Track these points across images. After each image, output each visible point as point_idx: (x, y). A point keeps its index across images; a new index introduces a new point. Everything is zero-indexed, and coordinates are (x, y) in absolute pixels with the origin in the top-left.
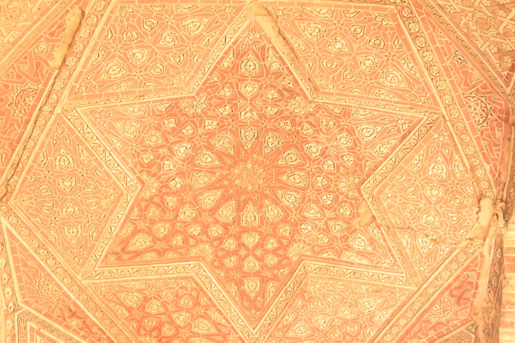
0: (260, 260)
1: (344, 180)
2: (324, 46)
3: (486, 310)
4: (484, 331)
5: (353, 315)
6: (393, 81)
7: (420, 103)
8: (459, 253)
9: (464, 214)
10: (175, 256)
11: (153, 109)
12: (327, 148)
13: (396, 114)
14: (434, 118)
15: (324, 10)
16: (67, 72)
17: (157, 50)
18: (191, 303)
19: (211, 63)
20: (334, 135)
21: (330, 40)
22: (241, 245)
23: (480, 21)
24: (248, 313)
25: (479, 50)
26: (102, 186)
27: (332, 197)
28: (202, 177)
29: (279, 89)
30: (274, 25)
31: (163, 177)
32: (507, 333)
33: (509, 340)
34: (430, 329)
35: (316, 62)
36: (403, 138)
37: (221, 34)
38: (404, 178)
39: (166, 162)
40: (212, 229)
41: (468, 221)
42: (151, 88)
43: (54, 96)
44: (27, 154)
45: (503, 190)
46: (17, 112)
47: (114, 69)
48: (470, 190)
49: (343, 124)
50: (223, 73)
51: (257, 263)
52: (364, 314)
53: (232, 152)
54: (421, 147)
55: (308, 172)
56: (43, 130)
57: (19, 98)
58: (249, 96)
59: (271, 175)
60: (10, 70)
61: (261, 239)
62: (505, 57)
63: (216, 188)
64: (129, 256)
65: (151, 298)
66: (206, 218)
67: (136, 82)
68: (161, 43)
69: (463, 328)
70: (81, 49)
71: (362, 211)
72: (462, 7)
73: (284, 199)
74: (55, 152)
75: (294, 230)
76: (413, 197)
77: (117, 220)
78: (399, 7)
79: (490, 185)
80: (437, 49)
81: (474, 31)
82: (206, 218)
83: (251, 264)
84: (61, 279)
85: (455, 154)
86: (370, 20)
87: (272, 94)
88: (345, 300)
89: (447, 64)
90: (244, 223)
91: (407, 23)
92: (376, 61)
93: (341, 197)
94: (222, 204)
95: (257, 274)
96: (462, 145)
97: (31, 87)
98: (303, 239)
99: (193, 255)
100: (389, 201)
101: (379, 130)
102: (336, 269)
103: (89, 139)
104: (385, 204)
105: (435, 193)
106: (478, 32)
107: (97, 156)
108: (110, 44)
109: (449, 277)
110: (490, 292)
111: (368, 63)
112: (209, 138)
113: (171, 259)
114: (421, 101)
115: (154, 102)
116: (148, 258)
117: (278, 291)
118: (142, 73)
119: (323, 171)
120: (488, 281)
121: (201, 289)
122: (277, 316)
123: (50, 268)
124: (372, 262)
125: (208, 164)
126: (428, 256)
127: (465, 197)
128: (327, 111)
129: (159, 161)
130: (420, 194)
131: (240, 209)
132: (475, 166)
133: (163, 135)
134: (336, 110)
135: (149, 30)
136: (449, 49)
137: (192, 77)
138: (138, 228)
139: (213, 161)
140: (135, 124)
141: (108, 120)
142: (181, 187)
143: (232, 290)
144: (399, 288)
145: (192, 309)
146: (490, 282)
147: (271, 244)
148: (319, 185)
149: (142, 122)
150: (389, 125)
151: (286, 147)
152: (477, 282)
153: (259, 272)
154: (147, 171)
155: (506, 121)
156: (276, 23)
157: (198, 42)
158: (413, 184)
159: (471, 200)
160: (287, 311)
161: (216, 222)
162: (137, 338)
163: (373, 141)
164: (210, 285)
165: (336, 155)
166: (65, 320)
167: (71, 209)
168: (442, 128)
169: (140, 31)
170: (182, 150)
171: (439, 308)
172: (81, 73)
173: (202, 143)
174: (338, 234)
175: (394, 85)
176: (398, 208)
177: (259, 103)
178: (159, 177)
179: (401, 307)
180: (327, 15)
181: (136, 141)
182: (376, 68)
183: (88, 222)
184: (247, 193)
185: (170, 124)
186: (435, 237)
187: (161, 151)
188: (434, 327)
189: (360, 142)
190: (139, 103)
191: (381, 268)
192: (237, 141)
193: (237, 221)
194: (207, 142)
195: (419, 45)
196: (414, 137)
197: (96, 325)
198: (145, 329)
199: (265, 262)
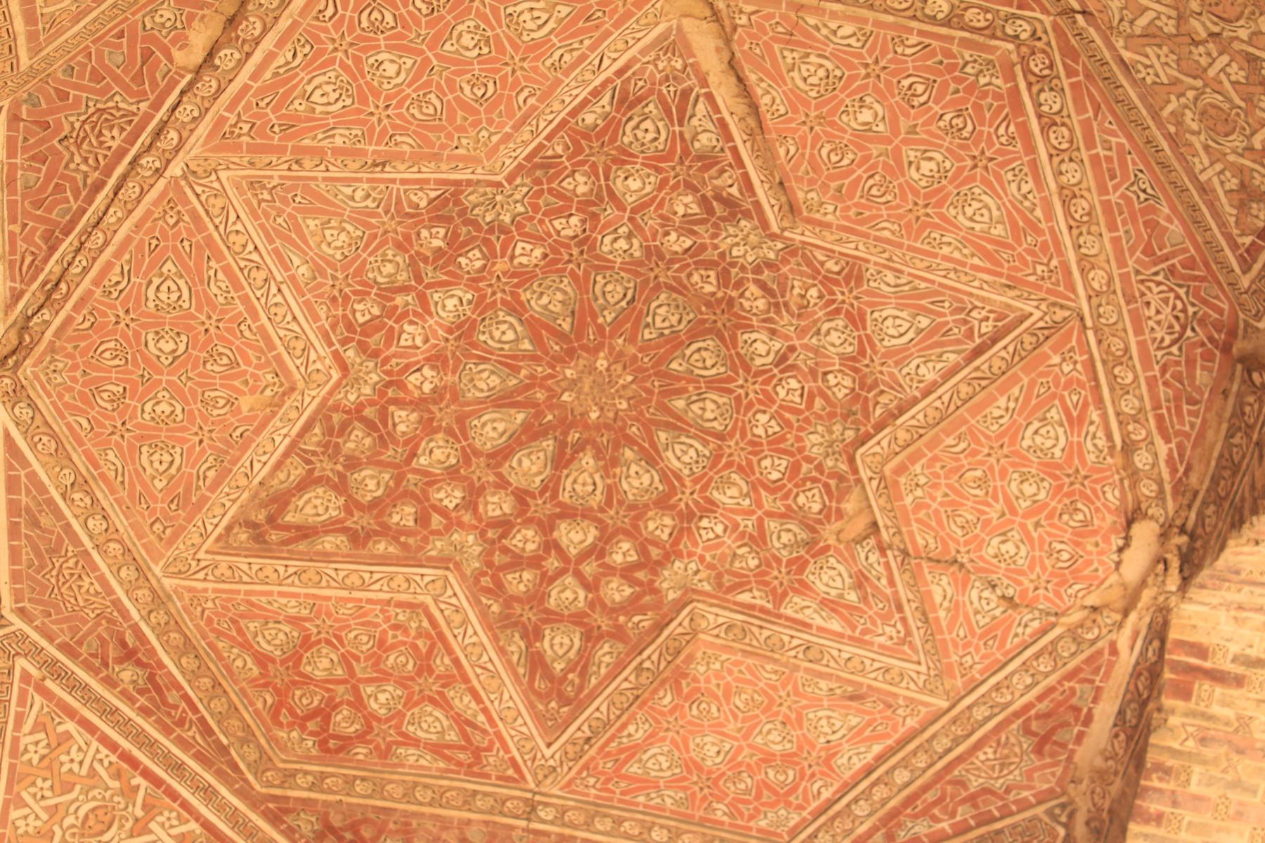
0: (590, 586)
1: (820, 428)
2: (832, 112)
3: (1101, 776)
4: (1087, 823)
5: (788, 746)
6: (977, 218)
7: (1032, 279)
8: (1060, 637)
10: (391, 549)
11: (399, 197)
12: (792, 349)
13: (971, 294)
14: (1058, 318)
15: (848, 29)
16: (214, 84)
17: (435, 62)
18: (410, 666)
19: (557, 111)
20: (816, 322)
21: (848, 101)
22: (551, 546)
23: (1212, 112)
24: (541, 707)
25: (1194, 178)
26: (248, 363)
27: (784, 463)
28: (485, 375)
29: (704, 196)
30: (721, 43)
31: (394, 361)
34: (964, 801)
35: (805, 147)
36: (978, 352)
37: (592, 48)
38: (963, 445)
39: (407, 327)
40: (490, 499)
41: (1096, 565)
42: (406, 148)
43: (173, 135)
44: (84, 263)
45: (1190, 507)
46: (77, 159)
47: (324, 93)
48: (1113, 496)
49: (840, 297)
50: (579, 139)
51: (582, 594)
52: (813, 746)
53: (566, 326)
54: (1015, 380)
55: (738, 399)
56: (130, 212)
57: (87, 127)
58: (630, 200)
59: (650, 392)
60: (79, 58)
61: (600, 539)
62: (1254, 205)
64: (285, 535)
65: (319, 642)
66: (480, 472)
67: (372, 129)
68: (447, 47)
69: (1039, 811)
70: (257, 33)
71: (849, 506)
72: (1176, 74)
73: (670, 454)
74: (151, 267)
75: (682, 529)
76: (977, 492)
77: (269, 448)
78: (1024, 49)
79: (1161, 491)
80: (1095, 160)
81: (1193, 133)
82: (480, 472)
83: (568, 594)
84: (114, 569)
85: (1092, 408)
86: (952, 68)
87: (685, 204)
89: (1114, 198)
90: (567, 495)
91: (1035, 89)
93: (805, 467)
94: (521, 444)
95: (578, 619)
96: (1112, 390)
97: (121, 105)
98: (699, 551)
99: (433, 553)
100: (919, 493)
101: (922, 326)
102: (766, 633)
103: (237, 248)
104: (908, 500)
105: (1029, 489)
106: (1202, 137)
107: (248, 290)
108: (326, 31)
109: (1028, 688)
110: (1116, 736)
111: (927, 167)
112: (517, 286)
113: (382, 556)
114: (1034, 273)
115: (404, 182)
116: (328, 546)
117: (619, 667)
118: (389, 112)
119: (773, 402)
120: (1116, 709)
122: (607, 724)
123: (91, 537)
124: (854, 628)
125: (507, 347)
126: (988, 632)
127: (1097, 510)
128: (809, 264)
129: (391, 323)
130: (995, 488)
131: (561, 460)
132: (1134, 442)
133: (412, 263)
134: (830, 265)
135: (425, 11)
136: (1123, 164)
137: (507, 138)
138: (317, 474)
139: (517, 340)
140: (349, 227)
141: (289, 210)
142: (434, 390)
143: (513, 648)
144: (905, 698)
145: (412, 679)
146: (1121, 713)
147: (624, 551)
148: (760, 431)
149: (367, 225)
150: (949, 318)
151: (698, 331)
152: (1090, 710)
154: (359, 342)
155: (1226, 349)
156: (728, 42)
157: (536, 59)
158: (982, 463)
159: (1110, 519)
160: (634, 715)
161: (502, 484)
162: (269, 730)
164: (461, 630)
166: (106, 665)
167: (164, 407)
168: (1074, 343)
169: (403, 11)
170: (451, 303)
171: (991, 756)
172: (246, 88)
173: (499, 295)
174: (784, 553)
175: (978, 227)
176: (936, 512)
177: (651, 221)
178: (386, 361)
180: (852, 41)
182: (944, 182)
183: (201, 442)
184: (586, 427)
185: (435, 238)
186: (1010, 592)
187: (399, 300)
188: (972, 799)
189: (873, 346)
190: (369, 180)
191: (872, 644)
192: (582, 300)
193: (551, 487)
194: (512, 293)
195: (1055, 143)
196: (1003, 354)
197: (179, 687)
198: (292, 712)
199: (602, 593)
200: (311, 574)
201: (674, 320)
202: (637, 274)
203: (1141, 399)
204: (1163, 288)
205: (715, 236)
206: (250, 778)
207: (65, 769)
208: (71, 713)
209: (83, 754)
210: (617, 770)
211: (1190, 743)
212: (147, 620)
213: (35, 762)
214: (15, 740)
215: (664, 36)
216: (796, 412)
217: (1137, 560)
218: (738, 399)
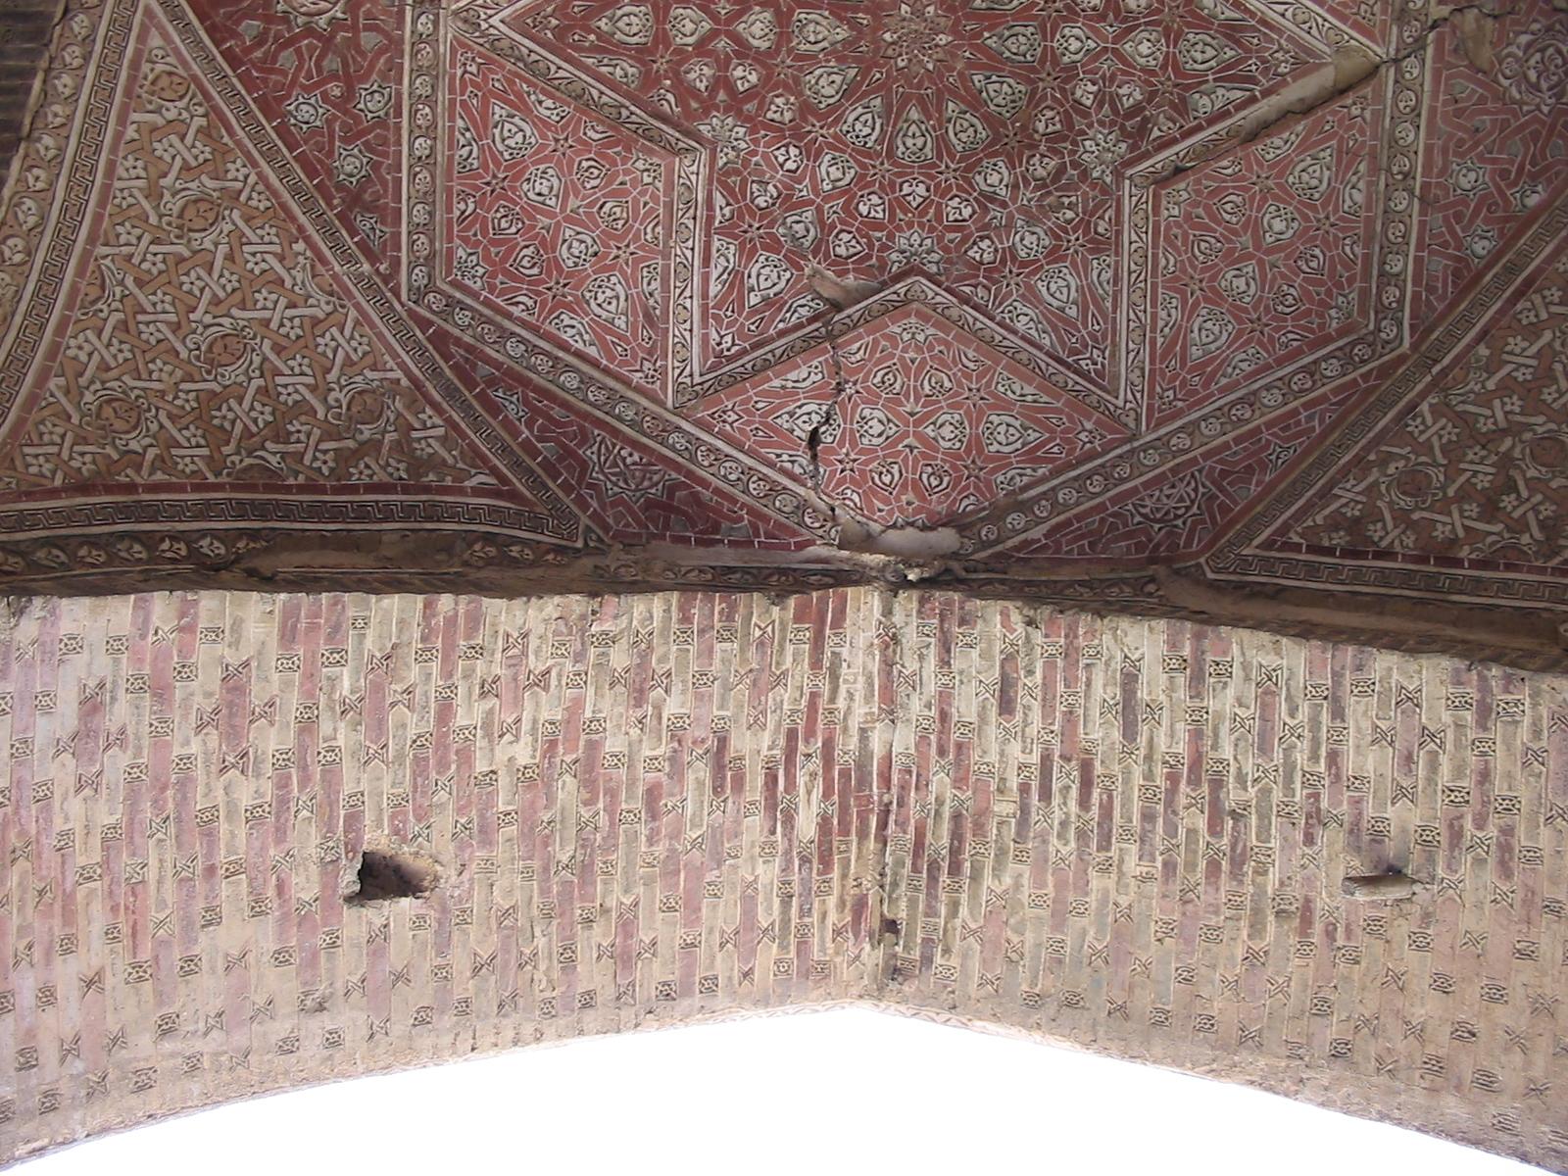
0: (702, 47)
2: (1276, 198)
6: (1204, 333)
7: (1158, 389)
8: (795, 495)
9: (904, 498)
14: (1123, 418)
15: (1359, 197)
27: (881, 215)
29: (1144, 108)
32: (668, 611)
33: (652, 617)
38: (971, 365)
48: (967, 504)
49: (1073, 238)
55: (934, 166)
69: (584, 520)
73: (860, 110)
75: (782, 130)
80: (1295, 412)
83: (689, 27)
86: (1340, 286)
88: (612, 243)
89: (1265, 436)
90: (803, 16)
92: (1247, 300)
95: (662, 39)
96: (1075, 479)
98: (761, 149)
105: (947, 431)
111: (1241, 283)
114: (1164, 391)
117: (614, 86)
127: (948, 495)
146: (731, 570)
147: (745, 76)
148: (906, 189)
158: (960, 385)
160: (564, 103)
163: (1041, 300)
165: (989, 224)
171: (629, 460)
179: (606, 371)
180: (1348, 202)
184: (875, 30)
201: (999, 100)
202: (1042, 61)
203: (1077, 504)
204: (1193, 495)
205: (1102, 123)
211: (758, 633)
215: (1310, 52)
218: (934, 166)
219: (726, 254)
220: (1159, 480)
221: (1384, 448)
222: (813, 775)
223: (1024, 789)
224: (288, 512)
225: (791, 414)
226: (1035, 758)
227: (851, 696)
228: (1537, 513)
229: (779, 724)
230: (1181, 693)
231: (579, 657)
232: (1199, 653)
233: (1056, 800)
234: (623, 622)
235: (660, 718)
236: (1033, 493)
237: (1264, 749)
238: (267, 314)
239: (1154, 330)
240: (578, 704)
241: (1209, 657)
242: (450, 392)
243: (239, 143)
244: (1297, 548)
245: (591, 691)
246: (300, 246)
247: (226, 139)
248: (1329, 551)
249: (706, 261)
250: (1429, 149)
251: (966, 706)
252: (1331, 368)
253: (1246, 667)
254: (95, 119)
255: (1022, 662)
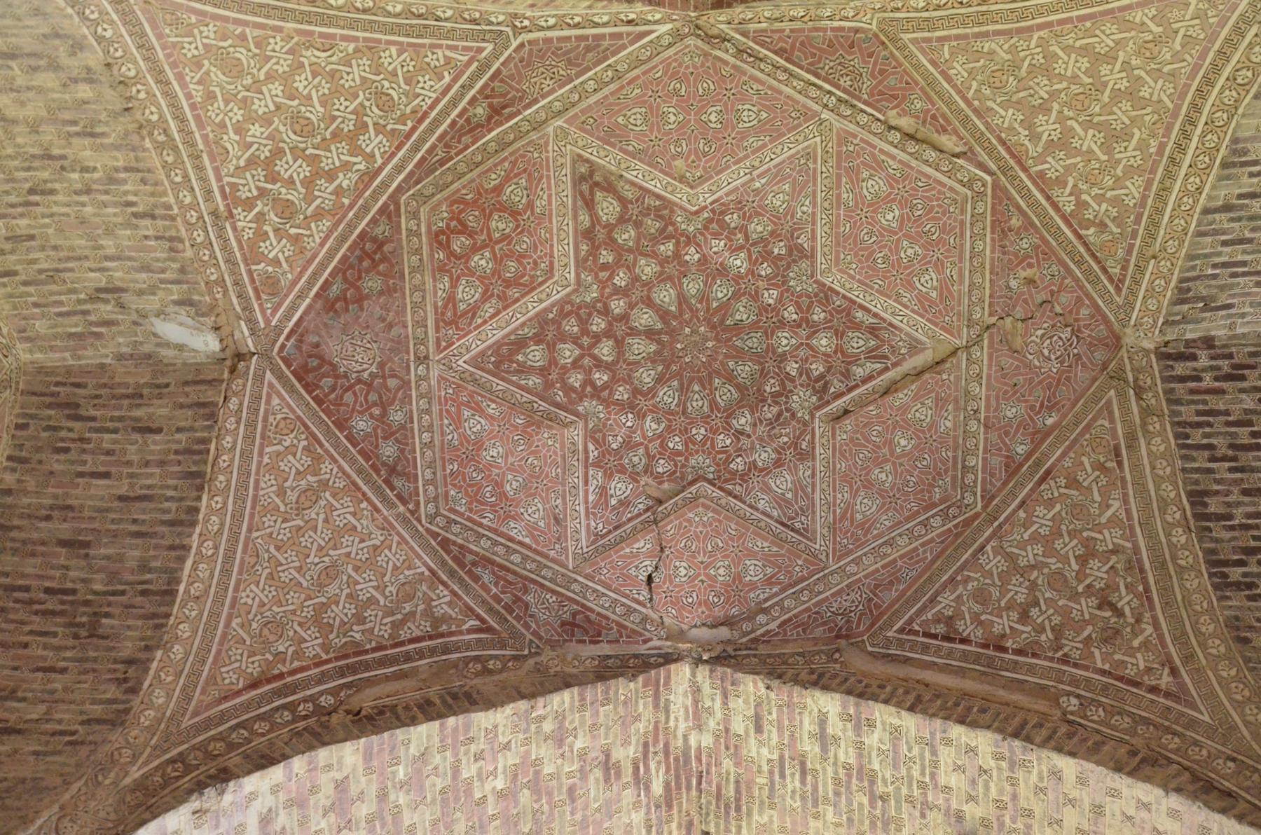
0: (575, 364)
2: (901, 427)
8: (640, 613)
15: (949, 424)
22: (597, 338)
26: (706, 162)
31: (702, 238)
32: (572, 698)
39: (722, 243)
43: (849, 112)
46: (832, 64)
47: (874, 186)
51: (569, 361)
53: (728, 322)
54: (782, 547)
55: (709, 416)
60: (894, 63)
63: (680, 304)
64: (587, 193)
65: (517, 220)
66: (636, 295)
69: (529, 636)
80: (916, 549)
83: (568, 353)
86: (939, 474)
89: (899, 563)
95: (553, 362)
104: (691, 515)
105: (721, 571)
111: (883, 476)
112: (750, 294)
121: (533, 289)
122: (491, 391)
128: (801, 434)
131: (650, 334)
136: (917, 562)
137: (853, 278)
145: (500, 277)
146: (609, 657)
147: (600, 377)
148: (694, 431)
153: (556, 365)
157: (902, 285)
161: (631, 306)
162: (446, 199)
163: (771, 490)
166: (487, 97)
167: (673, 118)
172: (875, 147)
179: (536, 552)
181: (760, 206)
185: (779, 249)
189: (767, 474)
193: (633, 332)
197: (473, 144)
198: (461, 212)
200: (564, 211)
201: (744, 375)
202: (767, 353)
205: (802, 385)
206: (411, 192)
207: (420, 78)
208: (455, 80)
209: (428, 88)
210: (462, 404)
212: (522, 120)
213: (427, 60)
214: (440, 46)
215: (916, 340)
216: (713, 446)
217: (704, 633)
218: (709, 416)
219: (597, 477)
220: (839, 593)
221: (966, 573)
222: (659, 763)
223: (771, 772)
224: (367, 666)
225: (636, 567)
226: (775, 757)
227: (677, 719)
228: (1050, 621)
229: (638, 741)
230: (850, 733)
231: (526, 731)
232: (858, 713)
233: (788, 780)
234: (549, 708)
235: (572, 752)
236: (770, 603)
237: (895, 766)
238: (348, 549)
239: (835, 505)
240: (528, 753)
241: (863, 716)
242: (452, 574)
243: (327, 451)
244: (916, 633)
245: (534, 746)
246: (364, 505)
247: (319, 450)
248: (935, 637)
249: (586, 483)
250: (988, 398)
251: (738, 726)
252: (936, 522)
253: (883, 723)
254: (246, 457)
255: (765, 708)
